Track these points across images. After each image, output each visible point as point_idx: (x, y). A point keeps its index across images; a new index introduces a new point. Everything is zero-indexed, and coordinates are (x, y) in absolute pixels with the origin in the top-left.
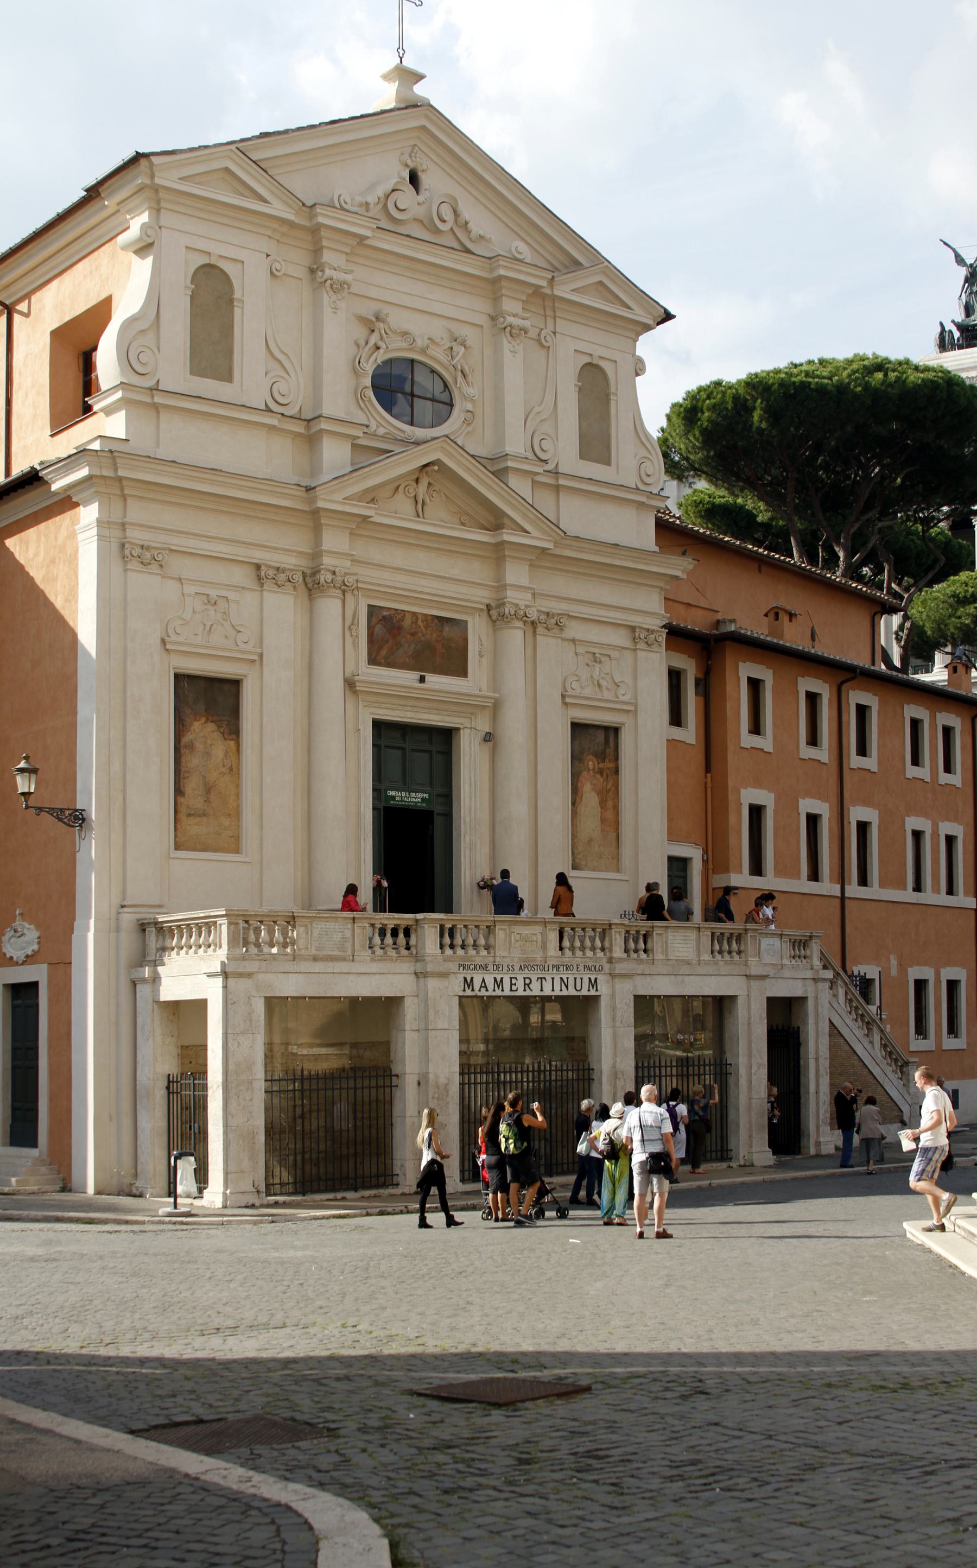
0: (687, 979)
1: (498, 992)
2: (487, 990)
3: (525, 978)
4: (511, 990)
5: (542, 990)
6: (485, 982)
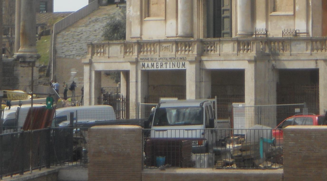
0: (224, 62)
1: (152, 69)
2: (149, 68)
3: (161, 63)
4: (156, 67)
5: (166, 67)
6: (149, 66)
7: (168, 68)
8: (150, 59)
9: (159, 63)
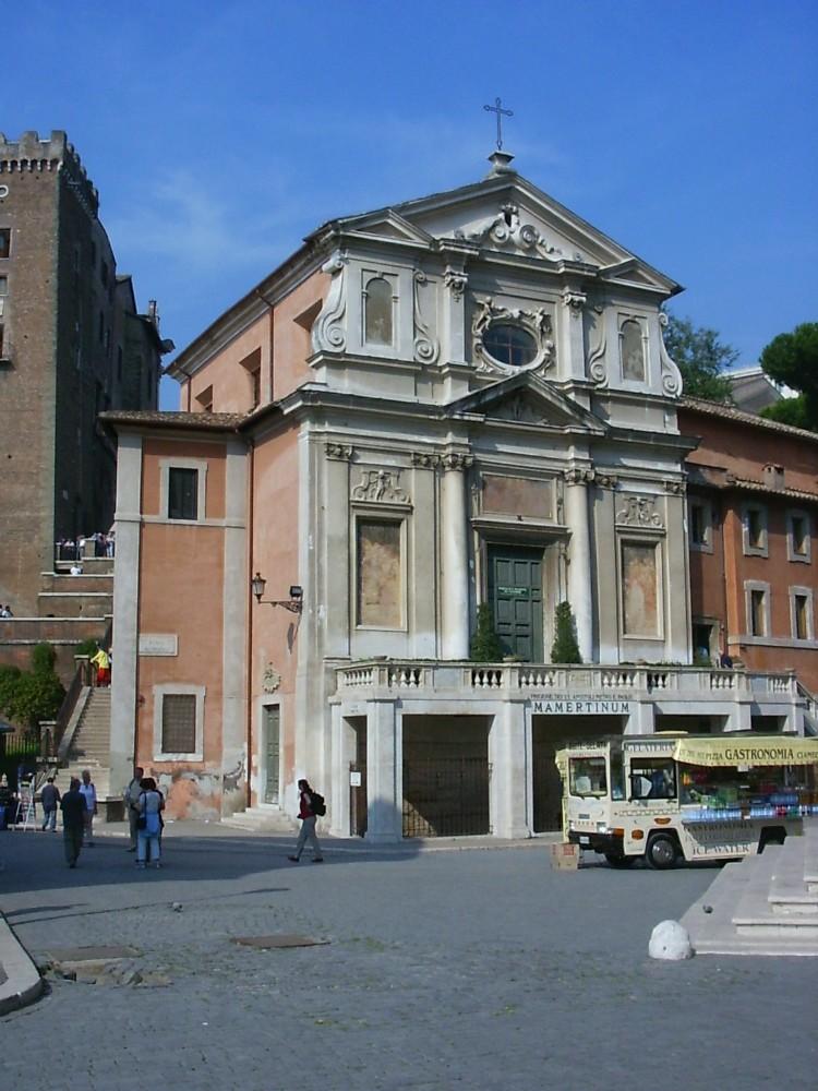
1: (559, 712)
7: (593, 712)
8: (554, 697)
9: (574, 703)
